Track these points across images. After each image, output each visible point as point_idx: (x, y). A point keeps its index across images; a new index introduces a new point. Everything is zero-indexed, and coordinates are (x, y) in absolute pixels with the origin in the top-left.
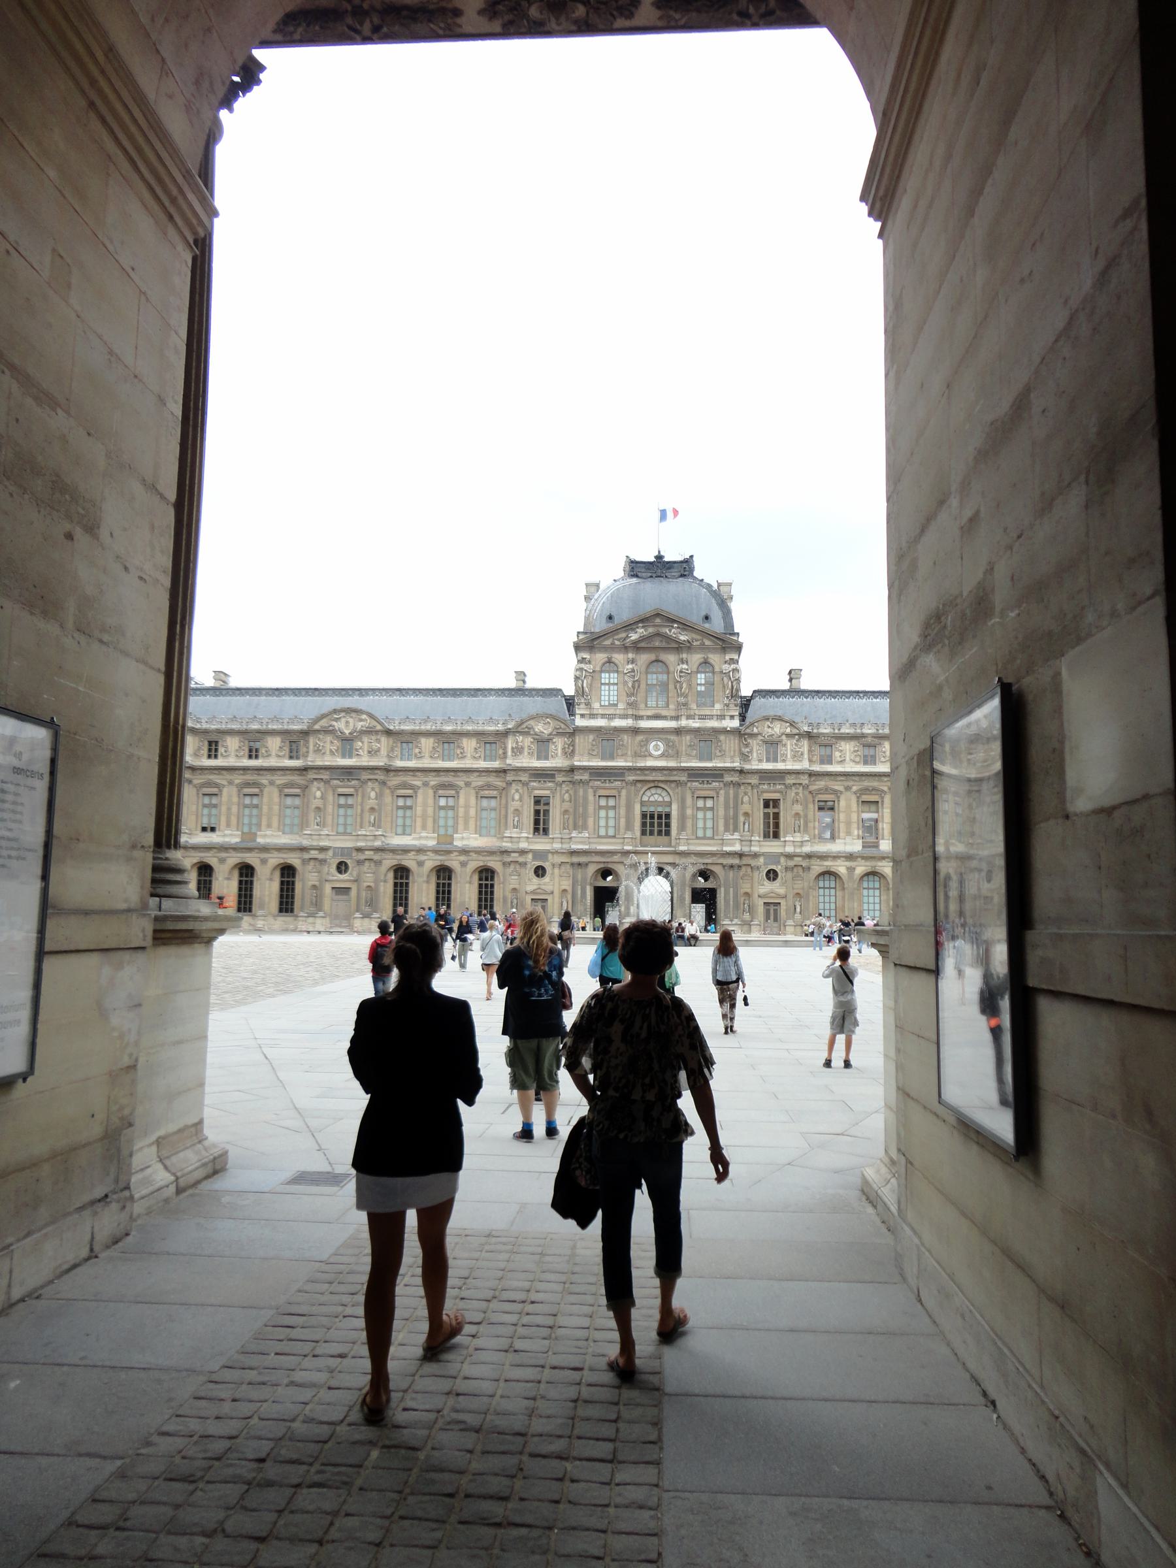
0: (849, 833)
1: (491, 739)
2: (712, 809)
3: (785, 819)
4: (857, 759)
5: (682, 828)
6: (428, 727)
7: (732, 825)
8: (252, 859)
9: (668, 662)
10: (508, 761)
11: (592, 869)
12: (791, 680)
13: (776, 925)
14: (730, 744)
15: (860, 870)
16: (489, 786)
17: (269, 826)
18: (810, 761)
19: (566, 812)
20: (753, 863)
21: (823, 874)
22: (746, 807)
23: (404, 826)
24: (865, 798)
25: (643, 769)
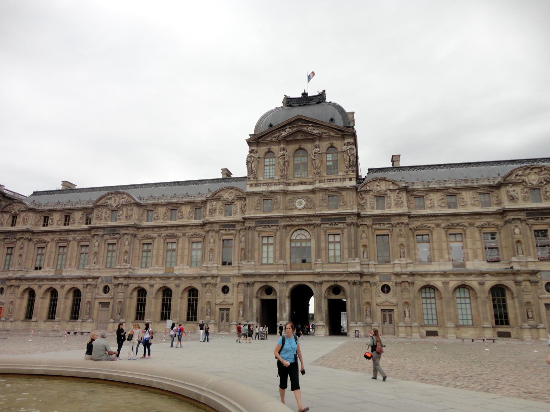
0: (441, 257)
1: (199, 205)
2: (339, 242)
4: (443, 205)
5: (318, 256)
6: (163, 201)
7: (354, 252)
8: (56, 285)
9: (307, 149)
10: (207, 218)
11: (257, 286)
12: (393, 165)
13: (391, 326)
14: (350, 197)
15: (453, 283)
16: (196, 235)
17: (70, 265)
18: (409, 208)
19: (242, 249)
20: (371, 280)
23: (146, 262)
24: (451, 231)
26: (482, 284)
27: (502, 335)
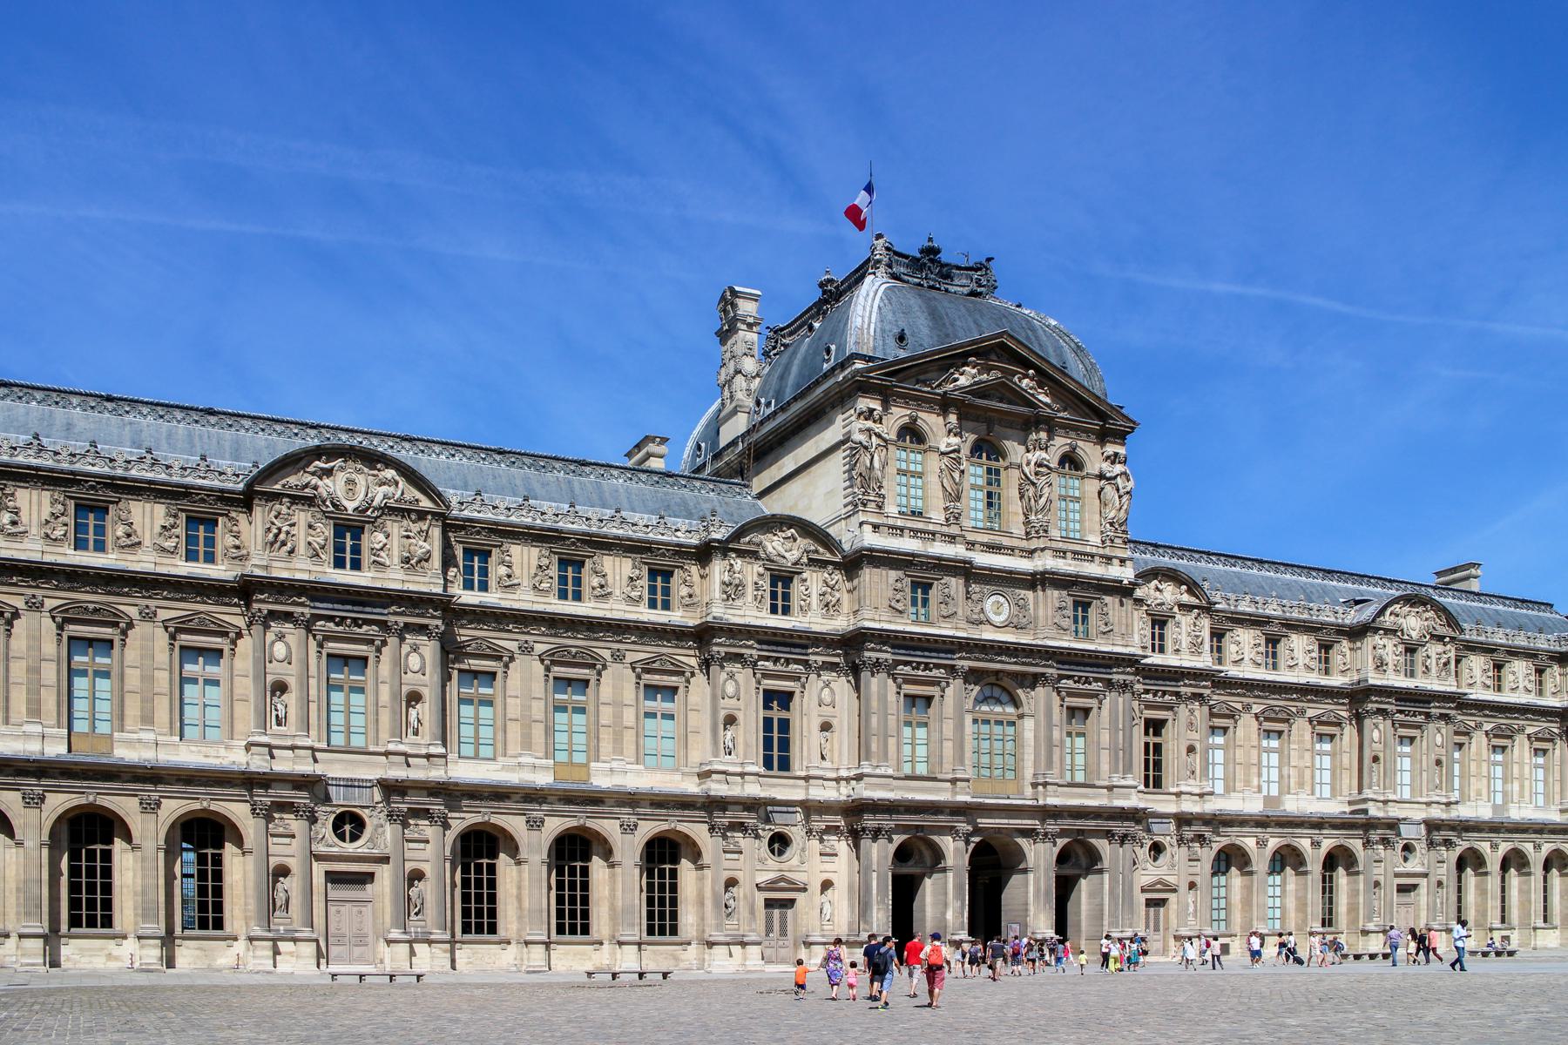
4: (1259, 659)
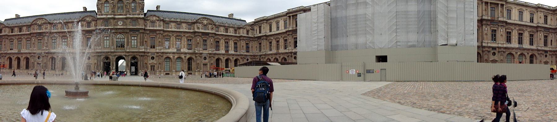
0: (173, 47)
3: (157, 43)
5: (128, 45)
7: (142, 44)
8: (20, 56)
11: (102, 57)
14: (142, 22)
15: (176, 57)
21: (166, 58)
22: (146, 40)
25: (117, 29)
26: (185, 57)
27: (189, 74)
